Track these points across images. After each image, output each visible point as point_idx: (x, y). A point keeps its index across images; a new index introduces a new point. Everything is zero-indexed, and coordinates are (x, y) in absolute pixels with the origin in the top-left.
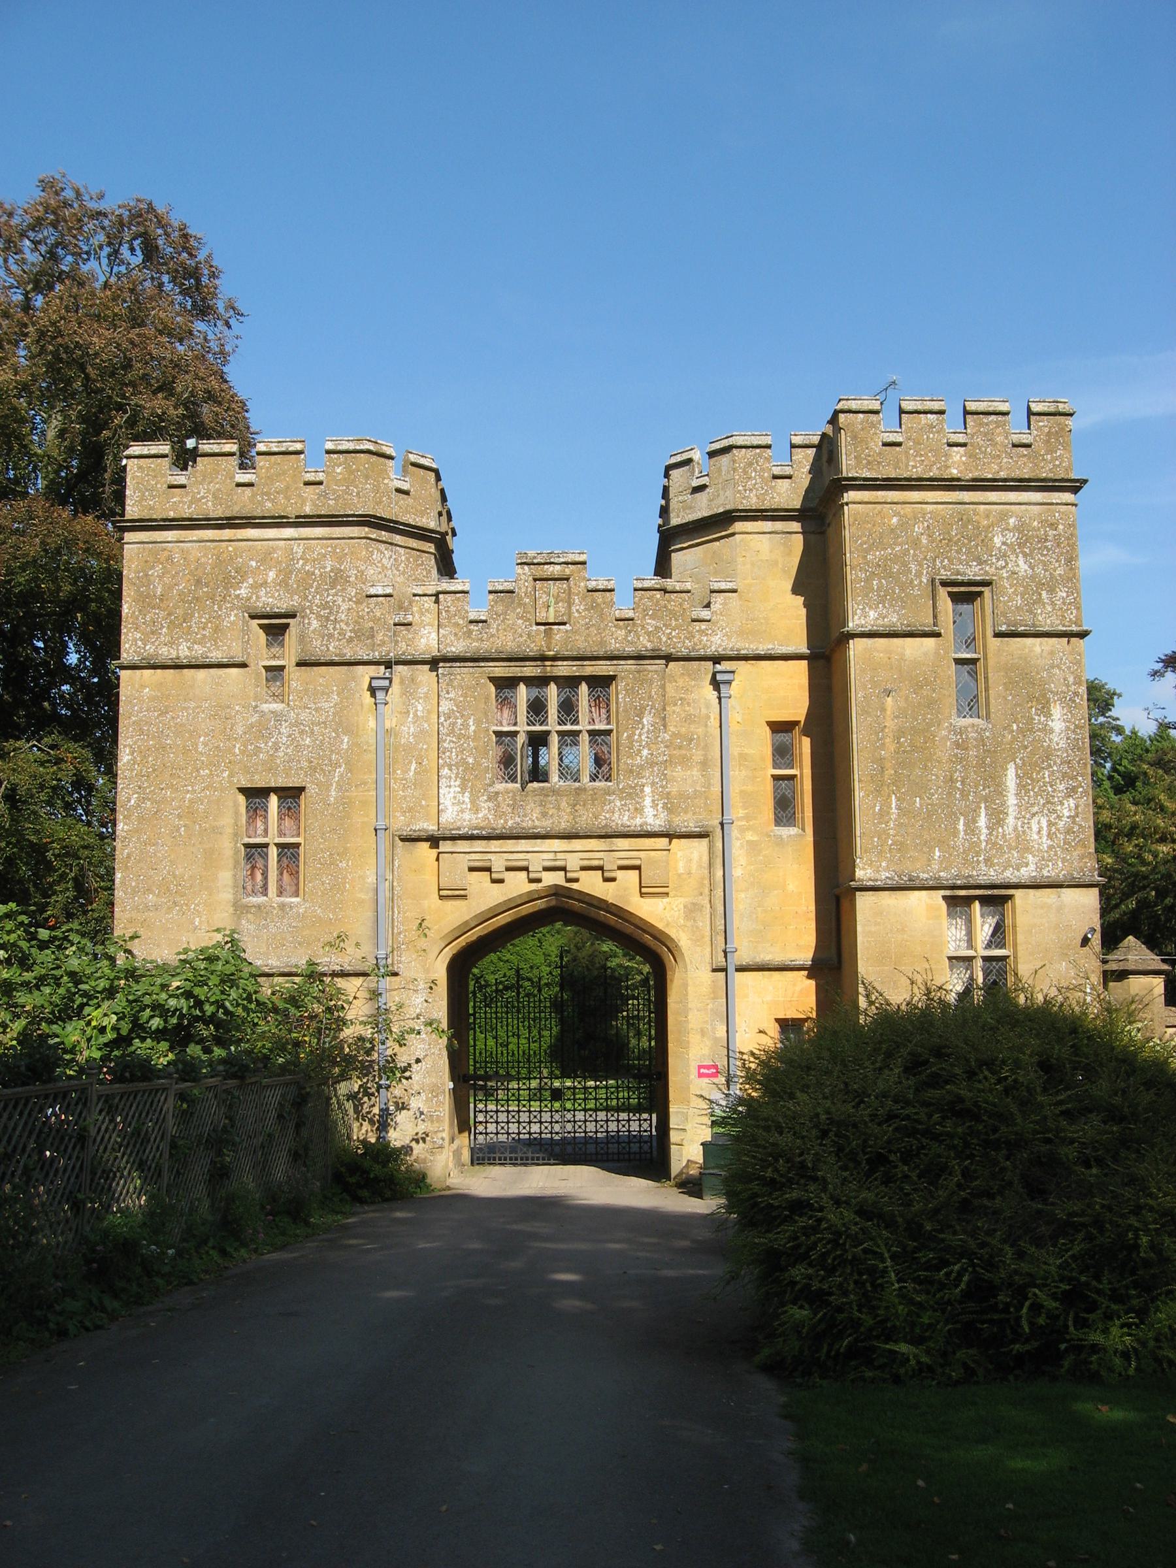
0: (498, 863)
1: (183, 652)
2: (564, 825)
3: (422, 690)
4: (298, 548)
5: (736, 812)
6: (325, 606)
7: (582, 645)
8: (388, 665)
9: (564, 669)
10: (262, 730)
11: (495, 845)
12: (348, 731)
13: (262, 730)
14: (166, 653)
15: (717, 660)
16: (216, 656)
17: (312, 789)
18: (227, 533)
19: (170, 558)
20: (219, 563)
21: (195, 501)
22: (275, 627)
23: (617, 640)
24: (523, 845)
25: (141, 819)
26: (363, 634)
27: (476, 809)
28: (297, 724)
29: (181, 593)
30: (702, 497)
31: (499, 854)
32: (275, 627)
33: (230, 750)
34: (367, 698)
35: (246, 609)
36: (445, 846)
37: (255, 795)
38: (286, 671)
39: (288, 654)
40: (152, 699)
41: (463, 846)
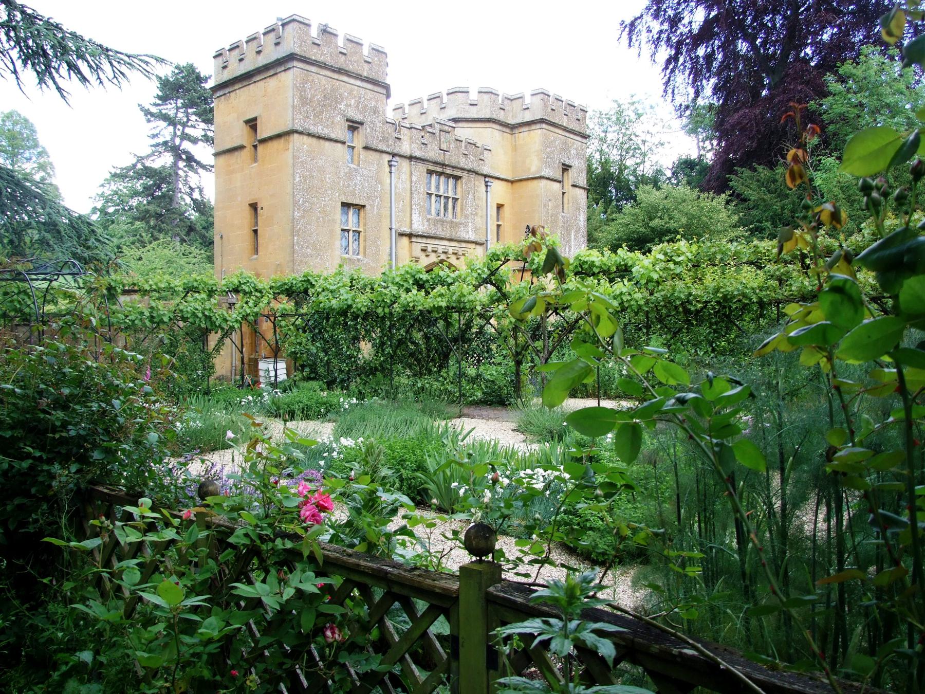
0: (430, 249)
1: (320, 130)
2: (448, 236)
3: (404, 170)
4: (362, 92)
5: (489, 237)
6: (372, 122)
7: (454, 162)
8: (394, 155)
9: (449, 171)
10: (350, 175)
11: (429, 241)
12: (380, 183)
13: (350, 175)
14: (313, 130)
15: (486, 176)
16: (333, 136)
17: (368, 207)
18: (336, 76)
19: (313, 80)
20: (333, 90)
21: (323, 54)
22: (354, 126)
23: (463, 163)
24: (437, 242)
25: (304, 211)
26: (385, 140)
27: (423, 225)
28: (363, 175)
29: (318, 100)
30: (474, 108)
31: (431, 244)
32: (354, 126)
33: (338, 183)
34: (387, 169)
35: (344, 116)
36: (414, 239)
37: (346, 205)
38: (356, 150)
39: (359, 141)
40: (308, 151)
41: (419, 240)
